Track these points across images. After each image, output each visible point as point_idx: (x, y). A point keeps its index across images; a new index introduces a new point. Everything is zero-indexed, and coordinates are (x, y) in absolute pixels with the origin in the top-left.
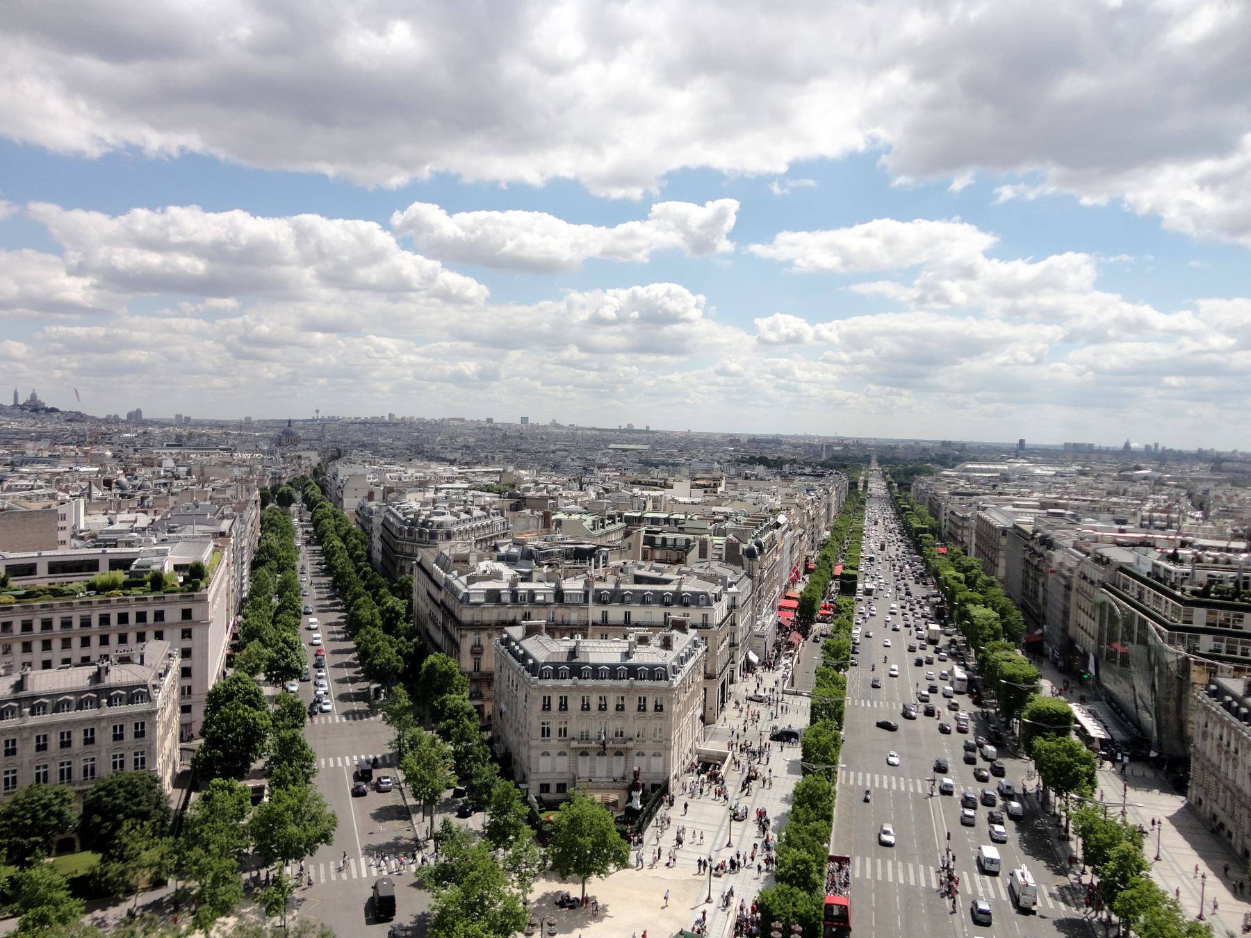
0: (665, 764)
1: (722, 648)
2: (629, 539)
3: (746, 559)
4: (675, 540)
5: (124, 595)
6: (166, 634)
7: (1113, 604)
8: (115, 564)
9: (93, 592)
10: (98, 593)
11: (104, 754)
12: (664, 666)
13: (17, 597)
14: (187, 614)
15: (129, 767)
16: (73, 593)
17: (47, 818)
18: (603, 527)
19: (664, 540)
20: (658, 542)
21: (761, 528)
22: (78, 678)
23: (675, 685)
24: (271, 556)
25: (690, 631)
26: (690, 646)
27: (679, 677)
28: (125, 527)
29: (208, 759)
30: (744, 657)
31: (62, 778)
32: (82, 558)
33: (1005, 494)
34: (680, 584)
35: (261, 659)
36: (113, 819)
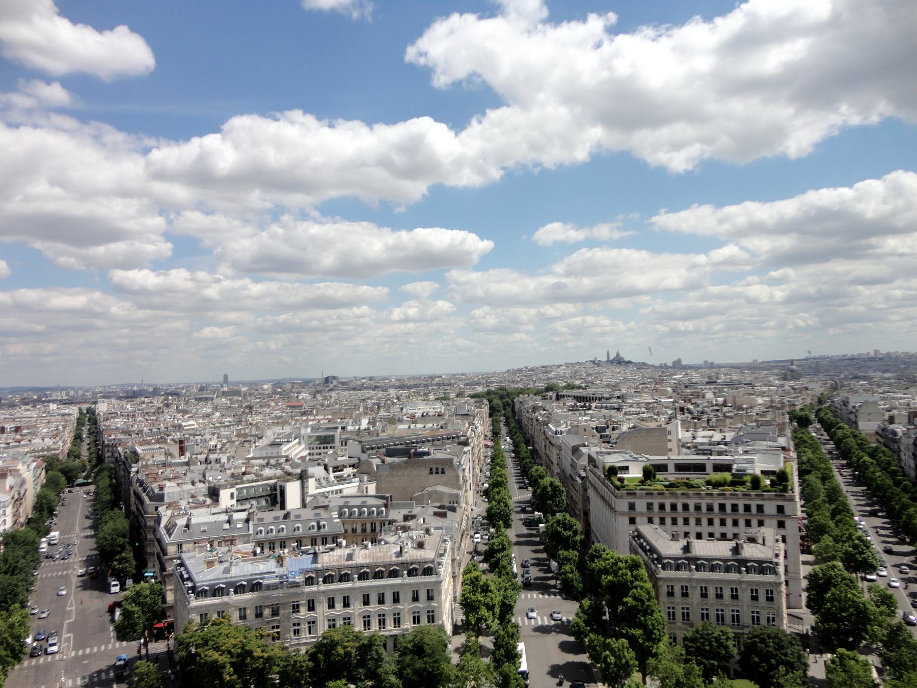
5: (734, 491)
6: (767, 522)
8: (718, 468)
9: (710, 487)
10: (713, 488)
11: (745, 609)
13: (665, 486)
14: (780, 509)
15: (764, 622)
16: (698, 487)
17: (718, 647)
22: (722, 549)
24: (812, 466)
28: (706, 440)
29: (825, 629)
31: (718, 620)
32: (695, 462)
35: (836, 551)
36: (768, 662)
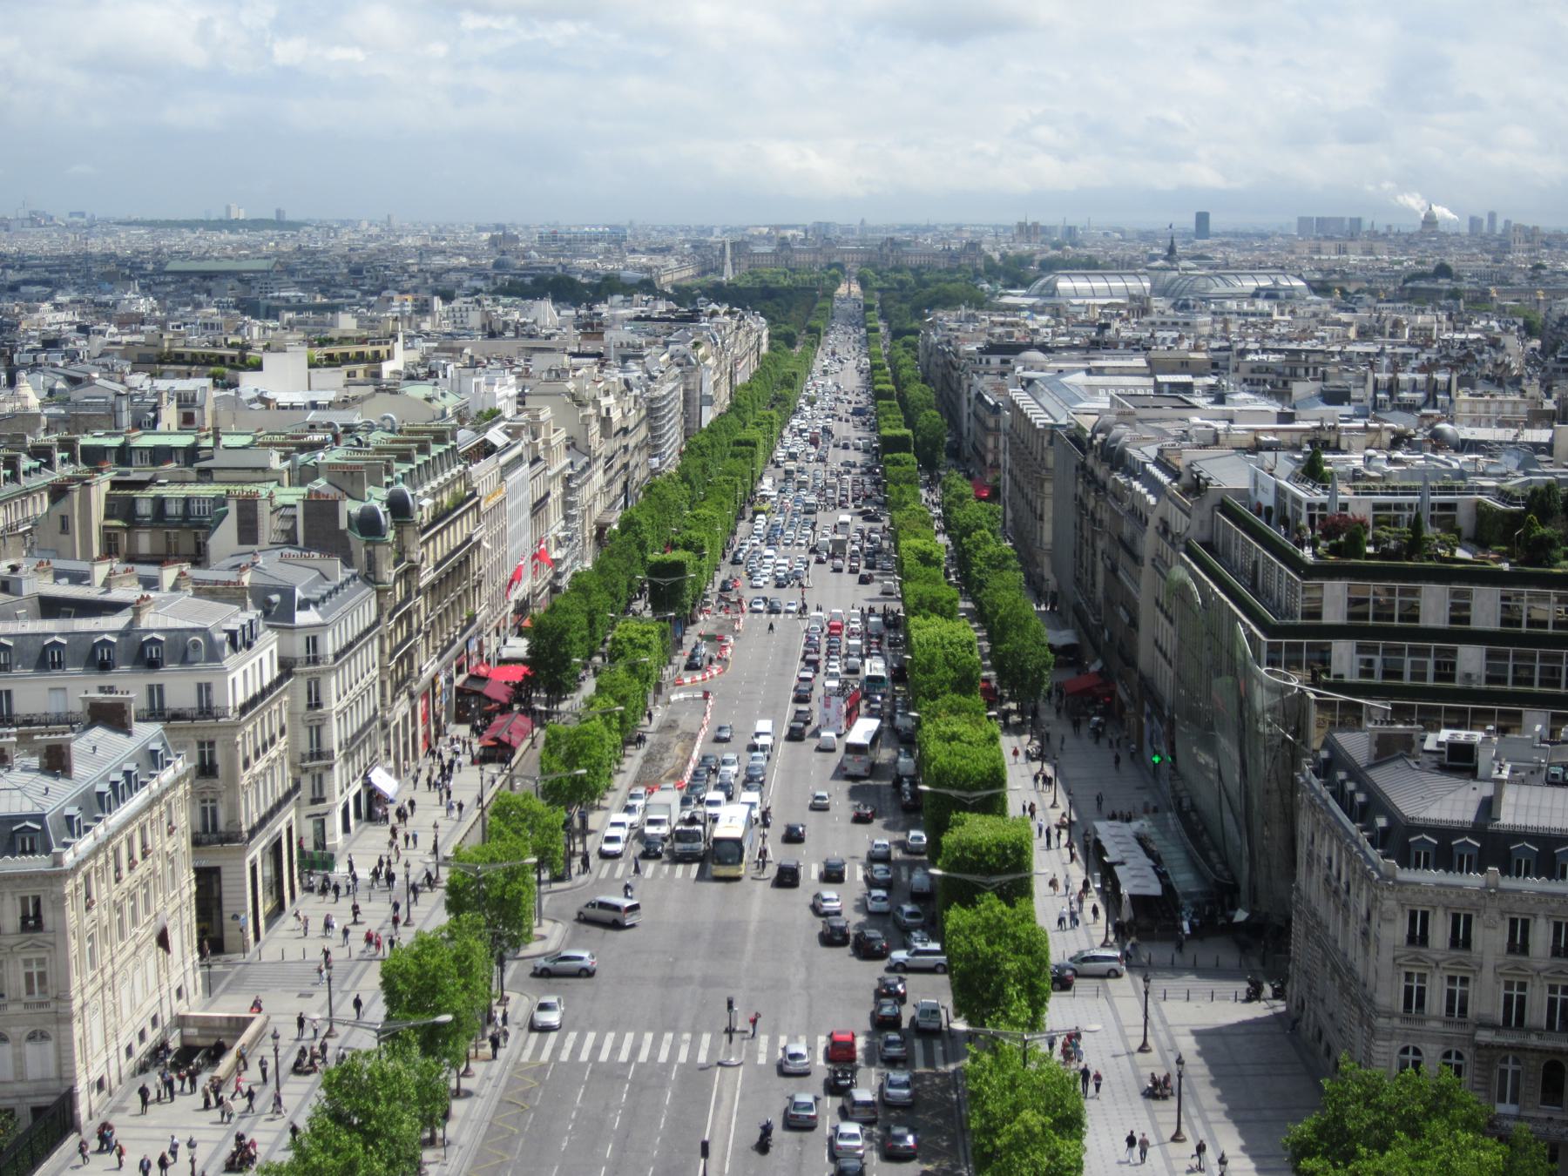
0: (59, 1057)
1: (258, 766)
2: (62, 506)
3: (356, 540)
4: (187, 501)
7: (1194, 587)
12: (39, 818)
18: (14, 478)
19: (160, 503)
20: (144, 508)
21: (420, 459)
23: (69, 858)
25: (137, 727)
26: (131, 766)
27: (85, 844)
30: (357, 786)
34: (137, 607)
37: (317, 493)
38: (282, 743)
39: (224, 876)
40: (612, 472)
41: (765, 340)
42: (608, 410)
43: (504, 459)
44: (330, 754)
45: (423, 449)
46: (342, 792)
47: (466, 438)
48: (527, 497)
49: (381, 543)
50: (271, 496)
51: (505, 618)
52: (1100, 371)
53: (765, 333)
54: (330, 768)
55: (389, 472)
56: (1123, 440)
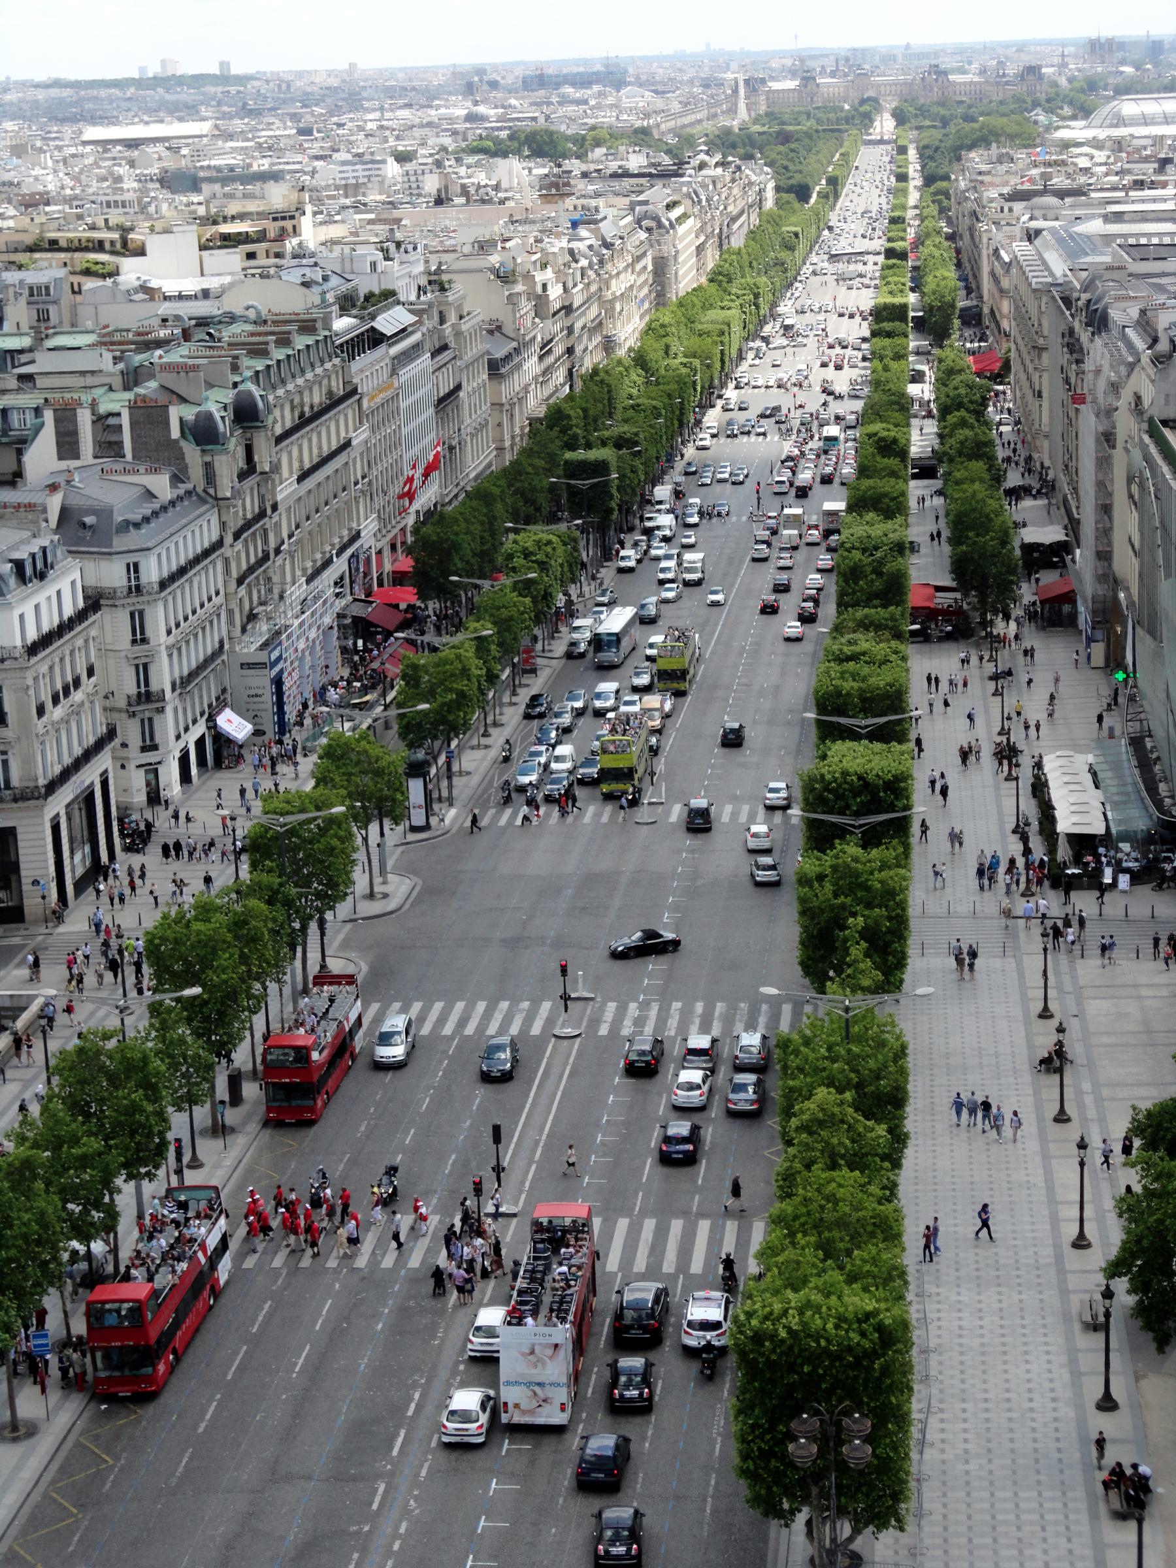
3: (193, 454)
21: (279, 354)
30: (200, 729)
33: (1153, 185)
37: (144, 398)
38: (88, 684)
39: (19, 837)
40: (550, 359)
41: (770, 194)
42: (544, 286)
43: (395, 350)
44: (161, 697)
45: (284, 341)
46: (178, 737)
47: (342, 324)
48: (427, 392)
49: (221, 452)
50: (94, 405)
51: (403, 530)
52: (1118, 217)
53: (771, 185)
54: (161, 710)
55: (235, 368)
56: (1106, 300)
